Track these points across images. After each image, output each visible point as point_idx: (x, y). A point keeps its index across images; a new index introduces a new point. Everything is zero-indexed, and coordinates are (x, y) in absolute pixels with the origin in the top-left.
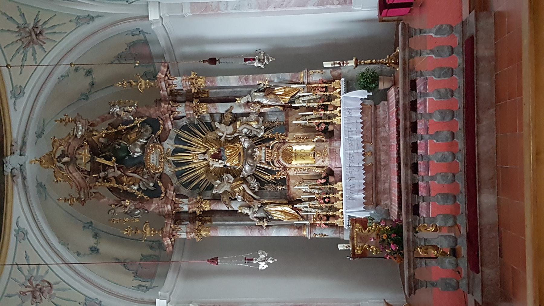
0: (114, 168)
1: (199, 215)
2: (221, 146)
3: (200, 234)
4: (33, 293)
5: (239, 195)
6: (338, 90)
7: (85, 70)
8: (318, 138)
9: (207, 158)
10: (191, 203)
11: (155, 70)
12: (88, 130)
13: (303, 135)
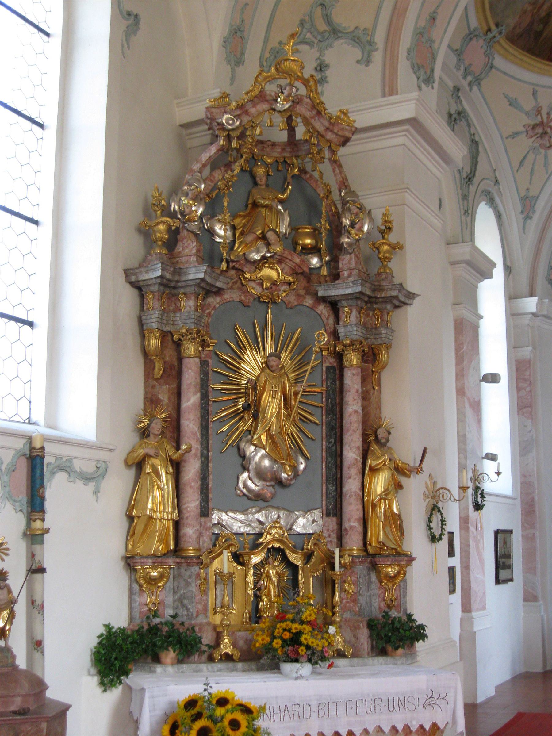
4: (542, 124)
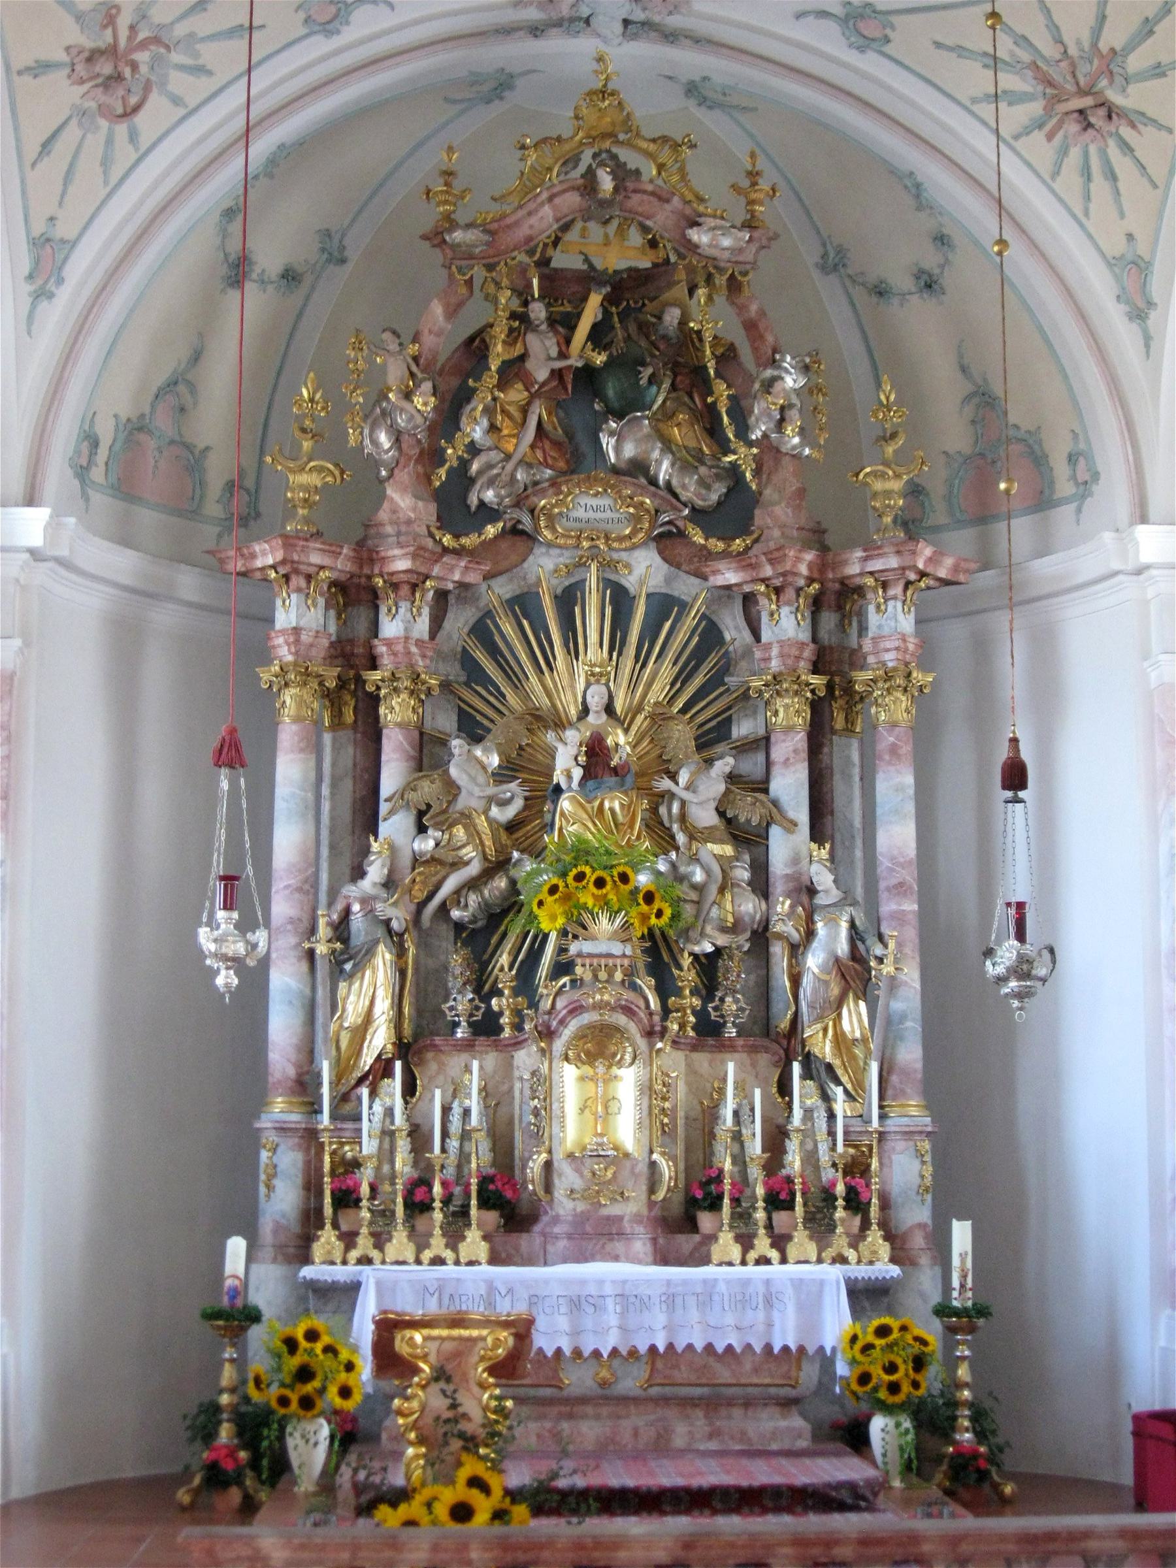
0: (563, 355)
1: (360, 681)
2: (639, 775)
3: (286, 685)
4: (112, 51)
5: (437, 845)
6: (851, 1255)
7: (936, 271)
8: (666, 1169)
9: (591, 718)
10: (414, 649)
11: (936, 529)
12: (716, 267)
13: (674, 1109)
